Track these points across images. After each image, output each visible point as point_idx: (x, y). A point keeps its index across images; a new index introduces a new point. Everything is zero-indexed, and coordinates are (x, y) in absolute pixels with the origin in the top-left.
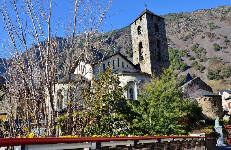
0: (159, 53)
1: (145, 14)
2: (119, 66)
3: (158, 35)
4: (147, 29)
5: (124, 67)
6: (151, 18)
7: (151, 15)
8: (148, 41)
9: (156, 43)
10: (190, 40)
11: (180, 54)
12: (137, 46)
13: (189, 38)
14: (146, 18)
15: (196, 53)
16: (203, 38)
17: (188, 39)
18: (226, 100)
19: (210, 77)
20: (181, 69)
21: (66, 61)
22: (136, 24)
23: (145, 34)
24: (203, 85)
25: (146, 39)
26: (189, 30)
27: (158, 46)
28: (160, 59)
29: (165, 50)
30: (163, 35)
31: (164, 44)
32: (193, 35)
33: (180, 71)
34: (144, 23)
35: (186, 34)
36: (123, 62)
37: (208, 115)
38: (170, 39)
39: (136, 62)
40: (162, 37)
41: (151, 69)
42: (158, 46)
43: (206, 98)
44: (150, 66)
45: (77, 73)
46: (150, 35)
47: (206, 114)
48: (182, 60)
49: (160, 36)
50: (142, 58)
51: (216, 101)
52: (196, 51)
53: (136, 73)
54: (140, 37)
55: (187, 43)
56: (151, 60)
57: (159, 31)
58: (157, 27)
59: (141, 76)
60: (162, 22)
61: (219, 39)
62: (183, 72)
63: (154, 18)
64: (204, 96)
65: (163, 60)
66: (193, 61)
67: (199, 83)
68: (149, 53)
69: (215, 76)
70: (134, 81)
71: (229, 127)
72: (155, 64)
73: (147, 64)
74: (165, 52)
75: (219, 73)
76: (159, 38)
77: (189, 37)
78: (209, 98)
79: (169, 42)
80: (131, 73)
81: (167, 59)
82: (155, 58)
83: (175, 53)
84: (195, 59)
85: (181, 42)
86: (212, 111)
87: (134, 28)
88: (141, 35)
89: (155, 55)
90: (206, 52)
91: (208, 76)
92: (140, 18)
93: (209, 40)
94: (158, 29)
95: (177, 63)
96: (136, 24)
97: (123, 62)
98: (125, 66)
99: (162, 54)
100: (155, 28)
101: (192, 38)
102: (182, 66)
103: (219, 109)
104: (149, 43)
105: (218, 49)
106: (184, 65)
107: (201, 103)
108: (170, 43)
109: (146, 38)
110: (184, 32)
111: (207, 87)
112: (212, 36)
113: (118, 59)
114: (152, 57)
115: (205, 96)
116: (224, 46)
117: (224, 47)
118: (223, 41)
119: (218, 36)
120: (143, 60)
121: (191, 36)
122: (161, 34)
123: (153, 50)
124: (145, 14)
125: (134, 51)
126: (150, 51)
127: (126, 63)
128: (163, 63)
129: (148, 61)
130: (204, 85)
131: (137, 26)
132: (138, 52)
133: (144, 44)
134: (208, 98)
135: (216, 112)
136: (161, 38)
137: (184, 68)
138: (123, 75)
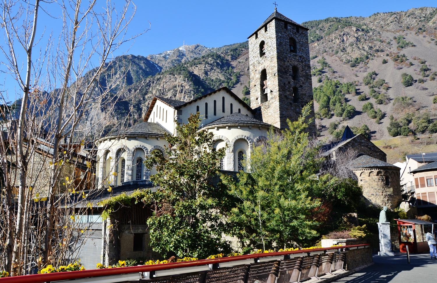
1: (274, 21)
2: (224, 111)
3: (294, 57)
4: (276, 47)
5: (234, 112)
6: (284, 27)
7: (283, 23)
8: (277, 68)
9: (290, 71)
10: (362, 66)
11: (344, 90)
12: (258, 76)
13: (361, 62)
14: (274, 28)
15: (371, 89)
16: (385, 62)
17: (359, 63)
18: (412, 174)
19: (393, 130)
20: (344, 115)
21: (146, 97)
22: (257, 37)
23: (272, 56)
24: (370, 148)
25: (273, 65)
26: (361, 47)
27: (295, 77)
28: (296, 99)
29: (307, 84)
30: (303, 59)
31: (304, 74)
32: (367, 58)
33: (341, 118)
34: (270, 36)
35: (356, 54)
36: (231, 105)
37: (373, 201)
38: (326, 63)
39: (255, 105)
40: (302, 62)
41: (280, 118)
42: (295, 77)
43: (372, 170)
44: (279, 112)
45: (152, 122)
46: (280, 58)
47: (370, 198)
48: (347, 100)
49: (298, 60)
50: (264, 97)
51: (390, 177)
52: (371, 85)
53: (250, 125)
54: (263, 61)
55: (357, 71)
56: (280, 101)
57: (298, 51)
58: (293, 42)
59: (260, 129)
60: (303, 35)
61: (412, 65)
62: (348, 121)
63: (288, 27)
64: (369, 167)
65: (303, 102)
66: (366, 102)
68: (278, 89)
69: (402, 130)
70: (246, 138)
71: (404, 223)
72: (287, 109)
73: (272, 108)
74: (306, 88)
75: (408, 125)
76: (296, 63)
77: (361, 61)
78: (378, 171)
79: (325, 68)
80: (242, 125)
82: (287, 98)
83: (334, 88)
84: (368, 99)
85: (347, 69)
86: (381, 194)
87: (254, 44)
88: (266, 57)
89: (288, 93)
90: (388, 88)
91: (390, 130)
92: (265, 26)
93: (395, 67)
94: (295, 47)
95: (338, 105)
96: (257, 37)
97: (231, 105)
98: (235, 110)
99: (300, 92)
100: (290, 46)
101: (365, 62)
102: (346, 111)
103: (393, 190)
104: (279, 71)
105: (409, 82)
106: (349, 109)
108: (326, 69)
109: (273, 62)
110: (352, 50)
111: (377, 152)
112: (399, 59)
113: (223, 98)
114: (283, 96)
115: (371, 168)
116: (421, 77)
117: (419, 80)
118: (419, 70)
119: (411, 60)
120: (267, 100)
121: (364, 58)
122: (300, 57)
123: (284, 84)
124: (274, 21)
125: (252, 84)
126: (279, 85)
127: (237, 106)
129: (275, 102)
130: (372, 149)
131: (259, 41)
132: (258, 87)
133: (269, 72)
134: (375, 171)
135: (388, 195)
137: (349, 115)
138: (227, 127)
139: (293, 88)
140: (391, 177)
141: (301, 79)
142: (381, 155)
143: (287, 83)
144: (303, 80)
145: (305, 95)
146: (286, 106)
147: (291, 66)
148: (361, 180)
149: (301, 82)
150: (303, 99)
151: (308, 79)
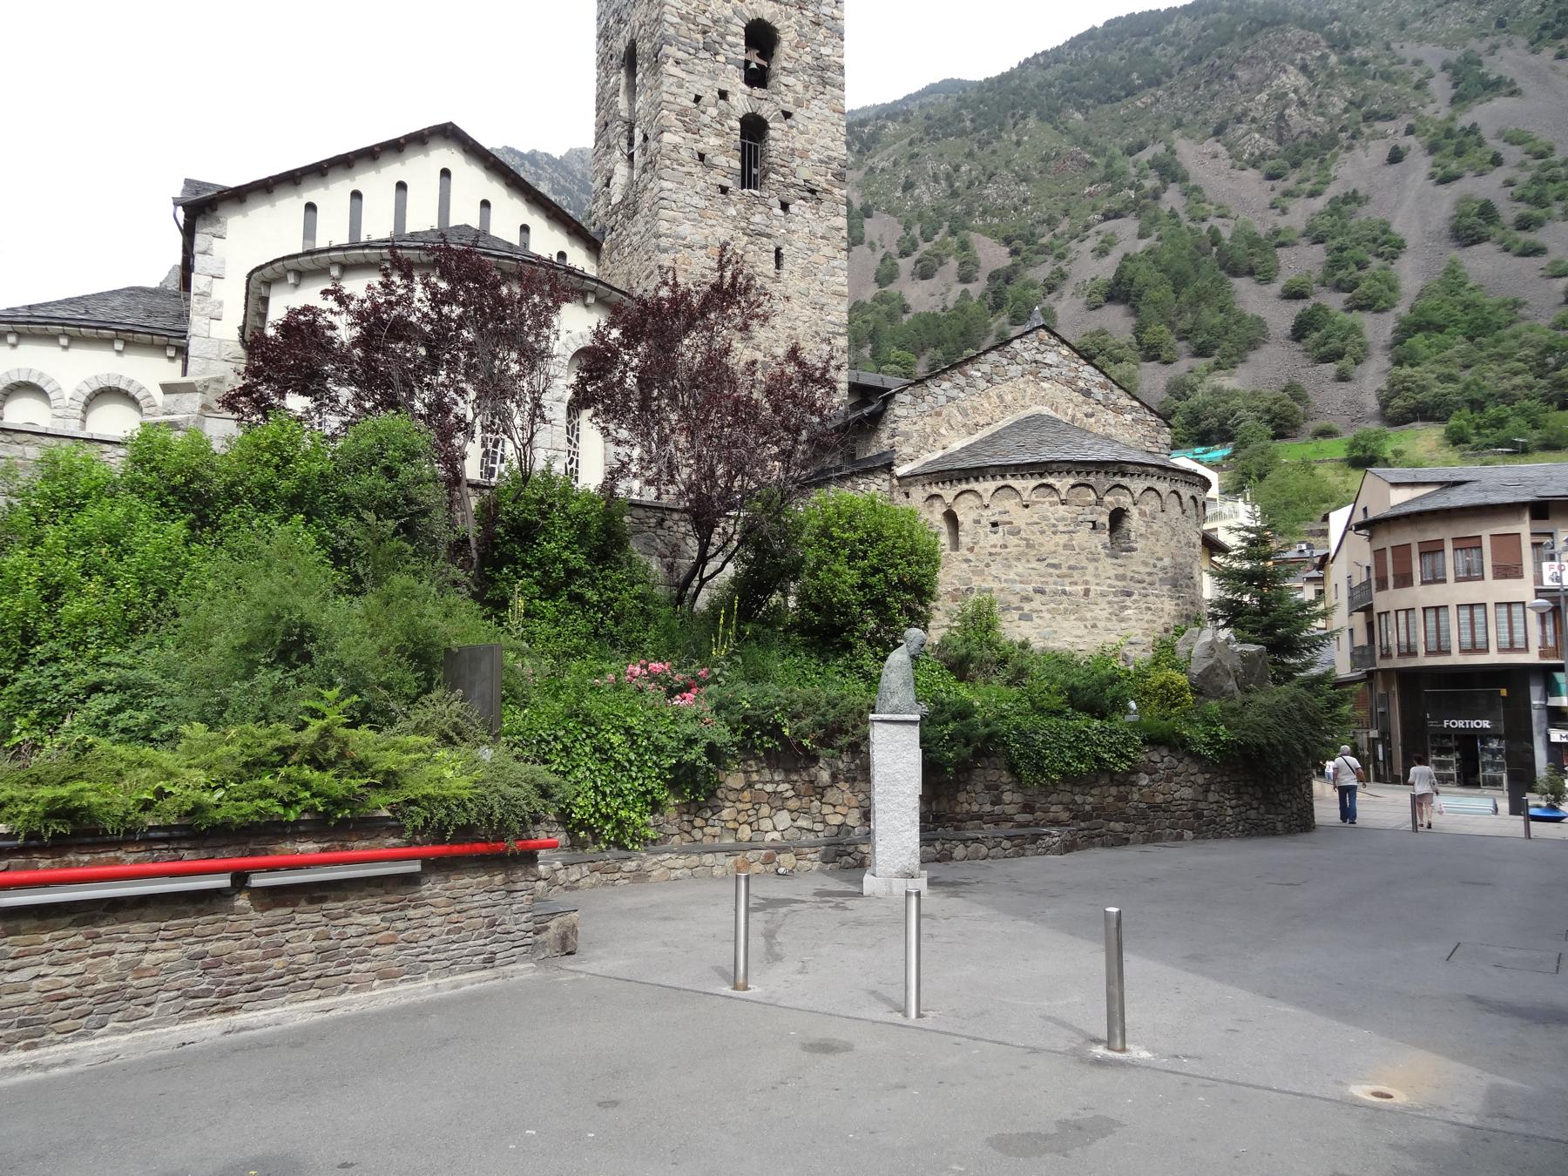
0: (754, 128)
31: (809, 59)
36: (485, 204)
51: (1134, 511)
67: (1046, 372)
74: (812, 127)
76: (767, 11)
78: (1072, 481)
81: (820, 182)
89: (714, 141)
97: (485, 204)
99: (778, 137)
107: (1005, 518)
113: (445, 173)
114: (685, 155)
123: (697, 99)
128: (778, 211)
136: (793, 11)
139: (742, 121)
140: (1142, 514)
141: (790, 80)
142: (1144, 422)
143: (710, 96)
144: (799, 87)
145: (804, 155)
146: (696, 200)
147: (736, 20)
148: (995, 525)
149: (790, 98)
150: (793, 173)
151: (824, 83)
